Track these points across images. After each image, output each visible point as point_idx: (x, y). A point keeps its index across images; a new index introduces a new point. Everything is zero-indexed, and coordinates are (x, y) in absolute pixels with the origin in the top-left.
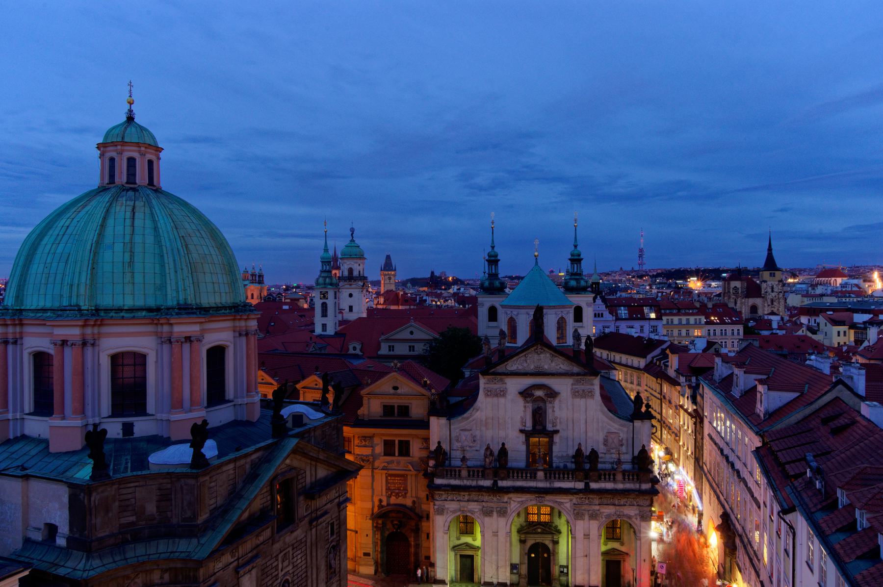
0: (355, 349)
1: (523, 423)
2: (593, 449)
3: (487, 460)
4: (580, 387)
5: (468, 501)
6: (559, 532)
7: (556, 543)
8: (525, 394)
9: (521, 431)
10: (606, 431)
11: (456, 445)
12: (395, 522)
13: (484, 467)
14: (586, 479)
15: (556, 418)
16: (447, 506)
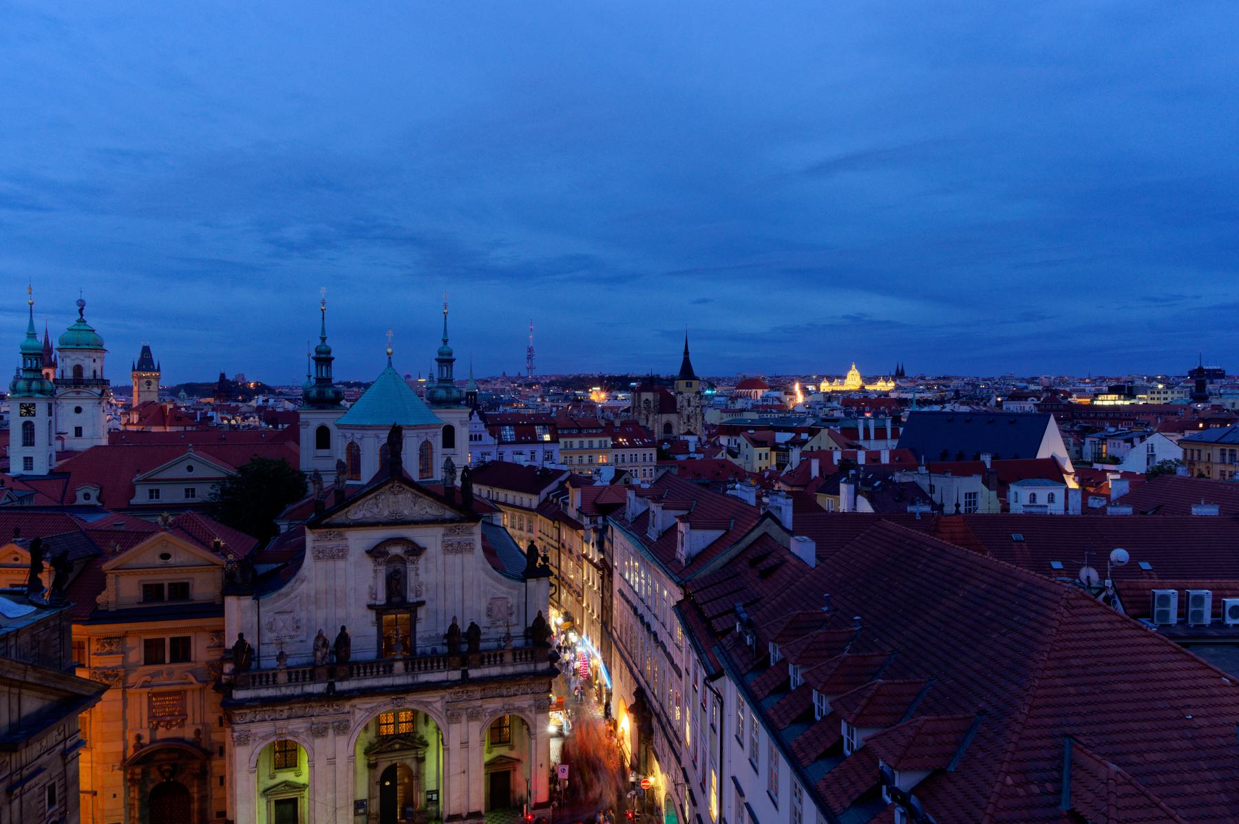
0: (87, 496)
1: (373, 595)
2: (472, 623)
3: (319, 654)
4: (455, 539)
5: (289, 718)
6: (426, 745)
7: (421, 760)
8: (376, 553)
9: (370, 607)
11: (268, 636)
13: (314, 665)
14: (463, 665)
16: (253, 731)
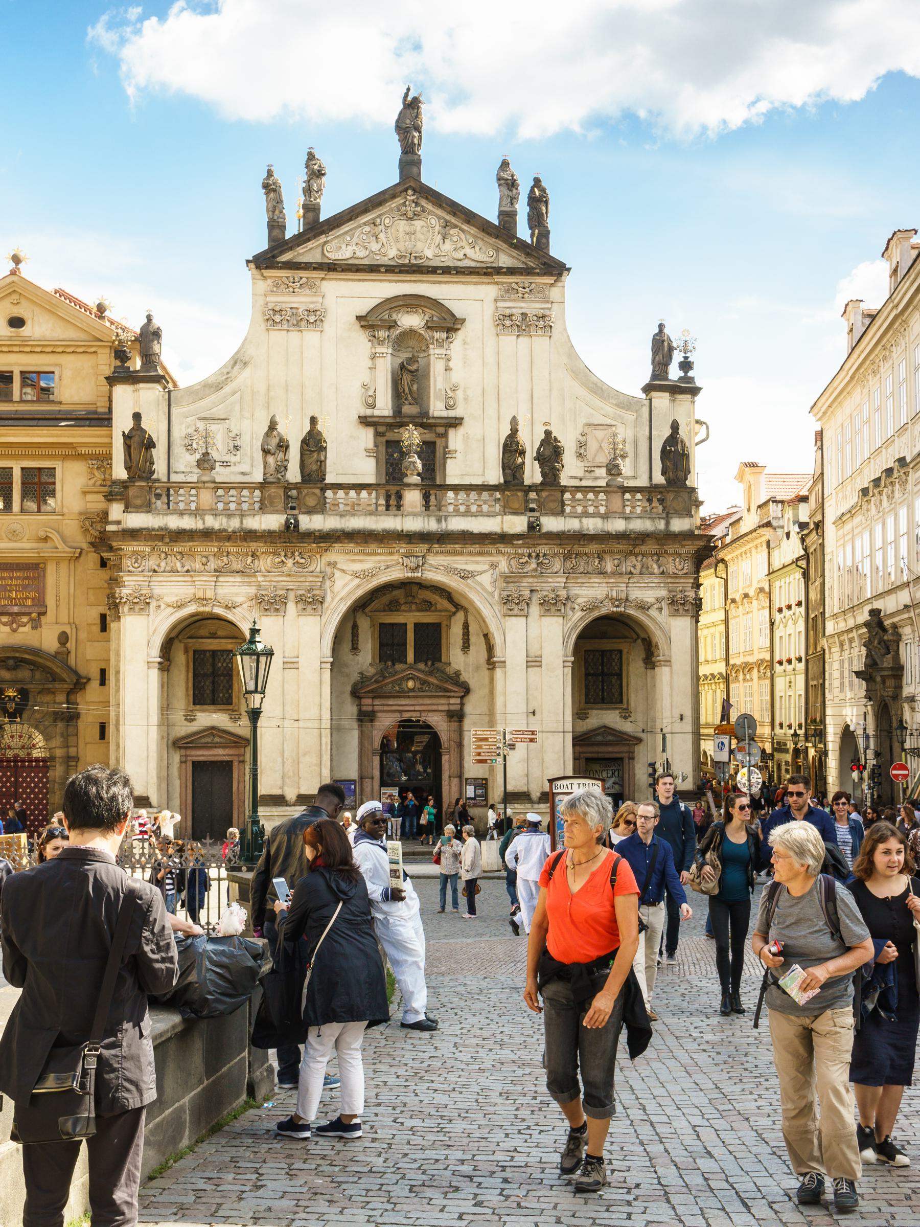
3: (271, 459)
4: (517, 307)
9: (365, 421)
10: (582, 421)
14: (532, 510)
16: (157, 590)
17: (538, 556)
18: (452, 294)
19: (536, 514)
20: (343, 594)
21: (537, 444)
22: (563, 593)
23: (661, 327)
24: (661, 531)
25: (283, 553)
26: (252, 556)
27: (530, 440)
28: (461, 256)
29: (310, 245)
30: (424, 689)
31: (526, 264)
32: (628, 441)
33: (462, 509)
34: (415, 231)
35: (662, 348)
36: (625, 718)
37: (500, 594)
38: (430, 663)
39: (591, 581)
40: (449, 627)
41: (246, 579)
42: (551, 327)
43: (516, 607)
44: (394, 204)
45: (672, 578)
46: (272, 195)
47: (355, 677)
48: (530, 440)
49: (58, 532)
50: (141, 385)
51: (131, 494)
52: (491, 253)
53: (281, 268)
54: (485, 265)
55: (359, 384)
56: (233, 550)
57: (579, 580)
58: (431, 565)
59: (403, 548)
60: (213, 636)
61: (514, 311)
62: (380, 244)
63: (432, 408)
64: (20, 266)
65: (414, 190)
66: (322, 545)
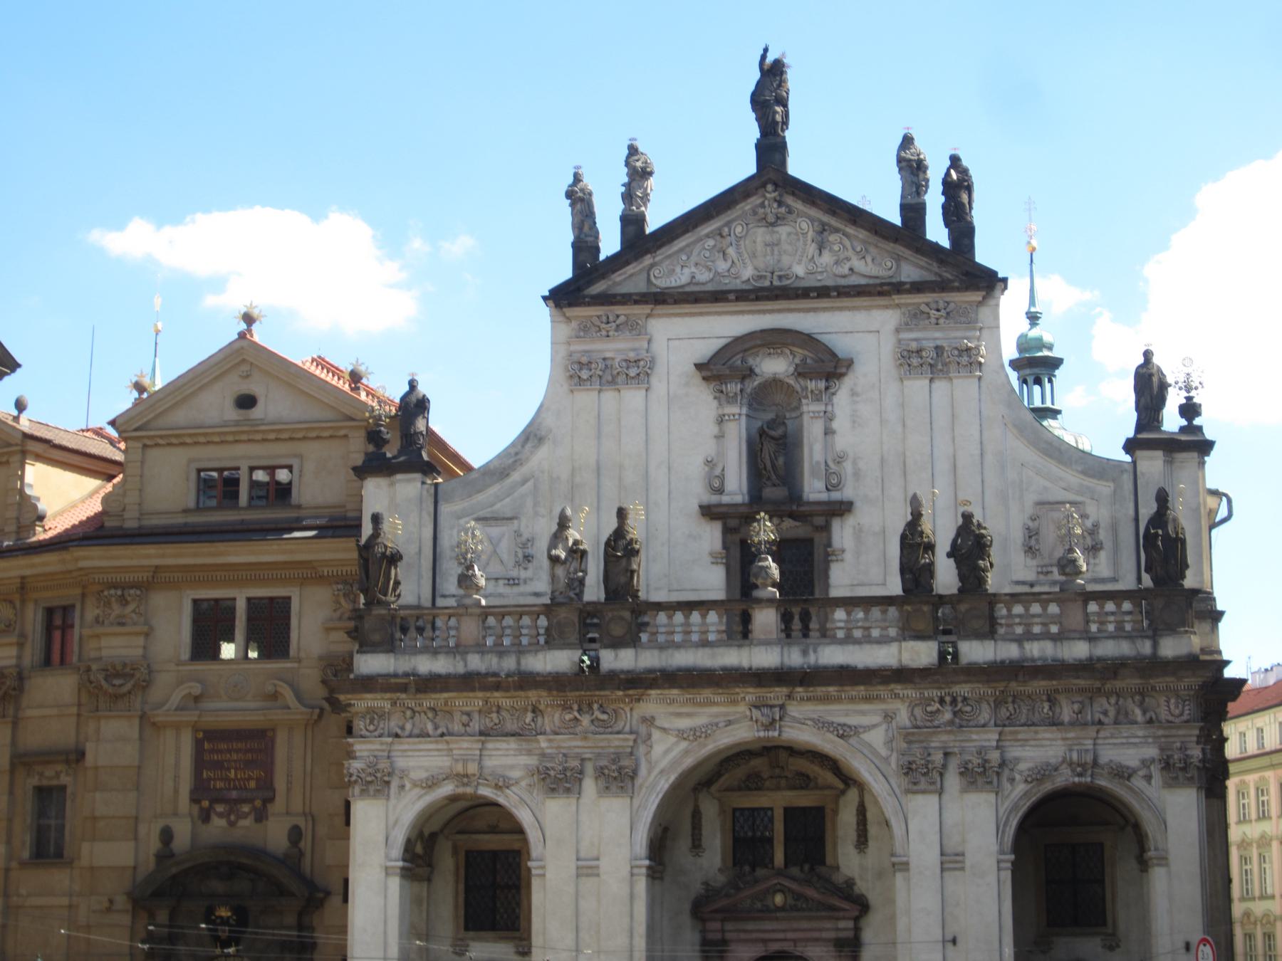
3: (560, 571)
6: (863, 906)
9: (709, 512)
10: (1031, 498)
12: (224, 913)
14: (946, 632)
15: (840, 459)
16: (401, 763)
17: (954, 701)
18: (836, 326)
19: (952, 638)
20: (664, 763)
21: (952, 535)
22: (994, 756)
23: (1148, 355)
24: (1145, 658)
25: (575, 707)
26: (534, 711)
27: (941, 530)
28: (846, 271)
29: (630, 269)
30: (798, 905)
31: (940, 276)
32: (1102, 525)
33: (858, 634)
34: (780, 240)
35: (1149, 388)
36: (1111, 948)
37: (898, 760)
38: (807, 867)
39: (1040, 736)
40: (835, 812)
41: (525, 745)
42: (980, 363)
43: (923, 779)
44: (747, 206)
45: (1165, 728)
46: (579, 206)
47: (697, 888)
48: (942, 530)
49: (291, 686)
50: (399, 476)
51: (367, 626)
52: (889, 264)
53: (589, 304)
54: (878, 281)
55: (699, 460)
56: (506, 702)
57: (1020, 737)
58: (795, 719)
59: (751, 694)
60: (493, 830)
61: (925, 344)
62: (729, 263)
63: (806, 488)
64: (255, 327)
65: (776, 185)
66: (631, 692)
